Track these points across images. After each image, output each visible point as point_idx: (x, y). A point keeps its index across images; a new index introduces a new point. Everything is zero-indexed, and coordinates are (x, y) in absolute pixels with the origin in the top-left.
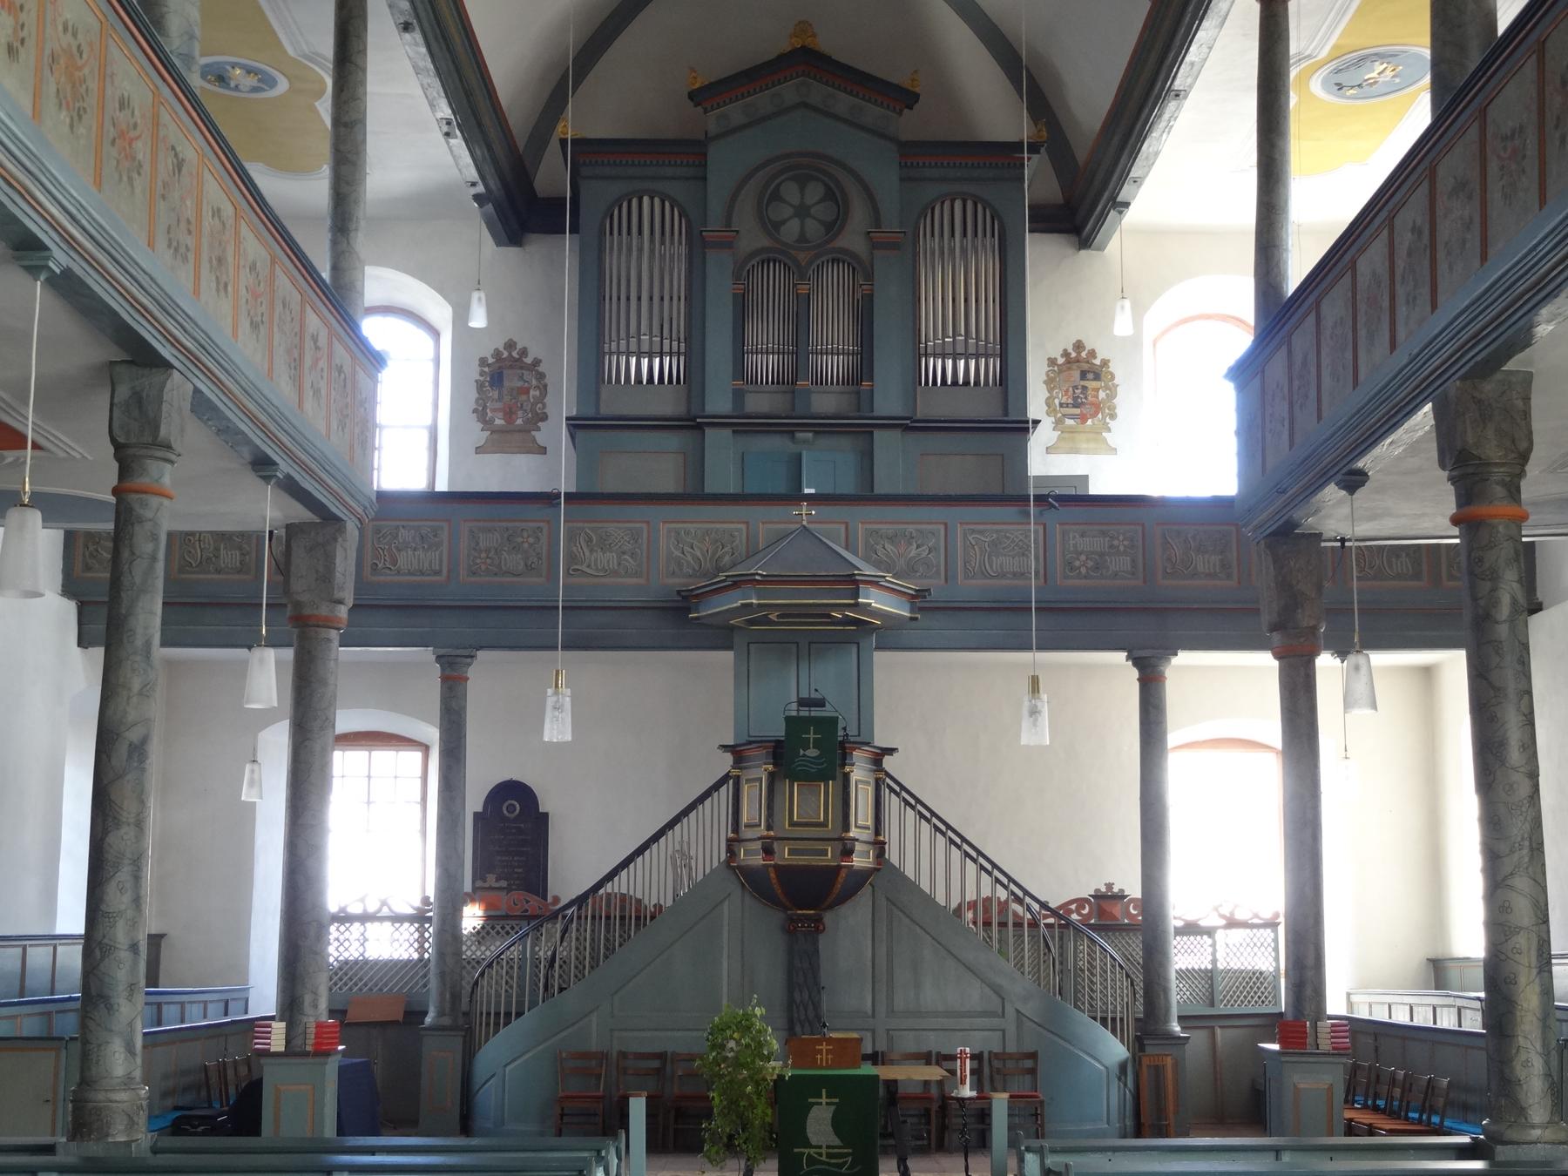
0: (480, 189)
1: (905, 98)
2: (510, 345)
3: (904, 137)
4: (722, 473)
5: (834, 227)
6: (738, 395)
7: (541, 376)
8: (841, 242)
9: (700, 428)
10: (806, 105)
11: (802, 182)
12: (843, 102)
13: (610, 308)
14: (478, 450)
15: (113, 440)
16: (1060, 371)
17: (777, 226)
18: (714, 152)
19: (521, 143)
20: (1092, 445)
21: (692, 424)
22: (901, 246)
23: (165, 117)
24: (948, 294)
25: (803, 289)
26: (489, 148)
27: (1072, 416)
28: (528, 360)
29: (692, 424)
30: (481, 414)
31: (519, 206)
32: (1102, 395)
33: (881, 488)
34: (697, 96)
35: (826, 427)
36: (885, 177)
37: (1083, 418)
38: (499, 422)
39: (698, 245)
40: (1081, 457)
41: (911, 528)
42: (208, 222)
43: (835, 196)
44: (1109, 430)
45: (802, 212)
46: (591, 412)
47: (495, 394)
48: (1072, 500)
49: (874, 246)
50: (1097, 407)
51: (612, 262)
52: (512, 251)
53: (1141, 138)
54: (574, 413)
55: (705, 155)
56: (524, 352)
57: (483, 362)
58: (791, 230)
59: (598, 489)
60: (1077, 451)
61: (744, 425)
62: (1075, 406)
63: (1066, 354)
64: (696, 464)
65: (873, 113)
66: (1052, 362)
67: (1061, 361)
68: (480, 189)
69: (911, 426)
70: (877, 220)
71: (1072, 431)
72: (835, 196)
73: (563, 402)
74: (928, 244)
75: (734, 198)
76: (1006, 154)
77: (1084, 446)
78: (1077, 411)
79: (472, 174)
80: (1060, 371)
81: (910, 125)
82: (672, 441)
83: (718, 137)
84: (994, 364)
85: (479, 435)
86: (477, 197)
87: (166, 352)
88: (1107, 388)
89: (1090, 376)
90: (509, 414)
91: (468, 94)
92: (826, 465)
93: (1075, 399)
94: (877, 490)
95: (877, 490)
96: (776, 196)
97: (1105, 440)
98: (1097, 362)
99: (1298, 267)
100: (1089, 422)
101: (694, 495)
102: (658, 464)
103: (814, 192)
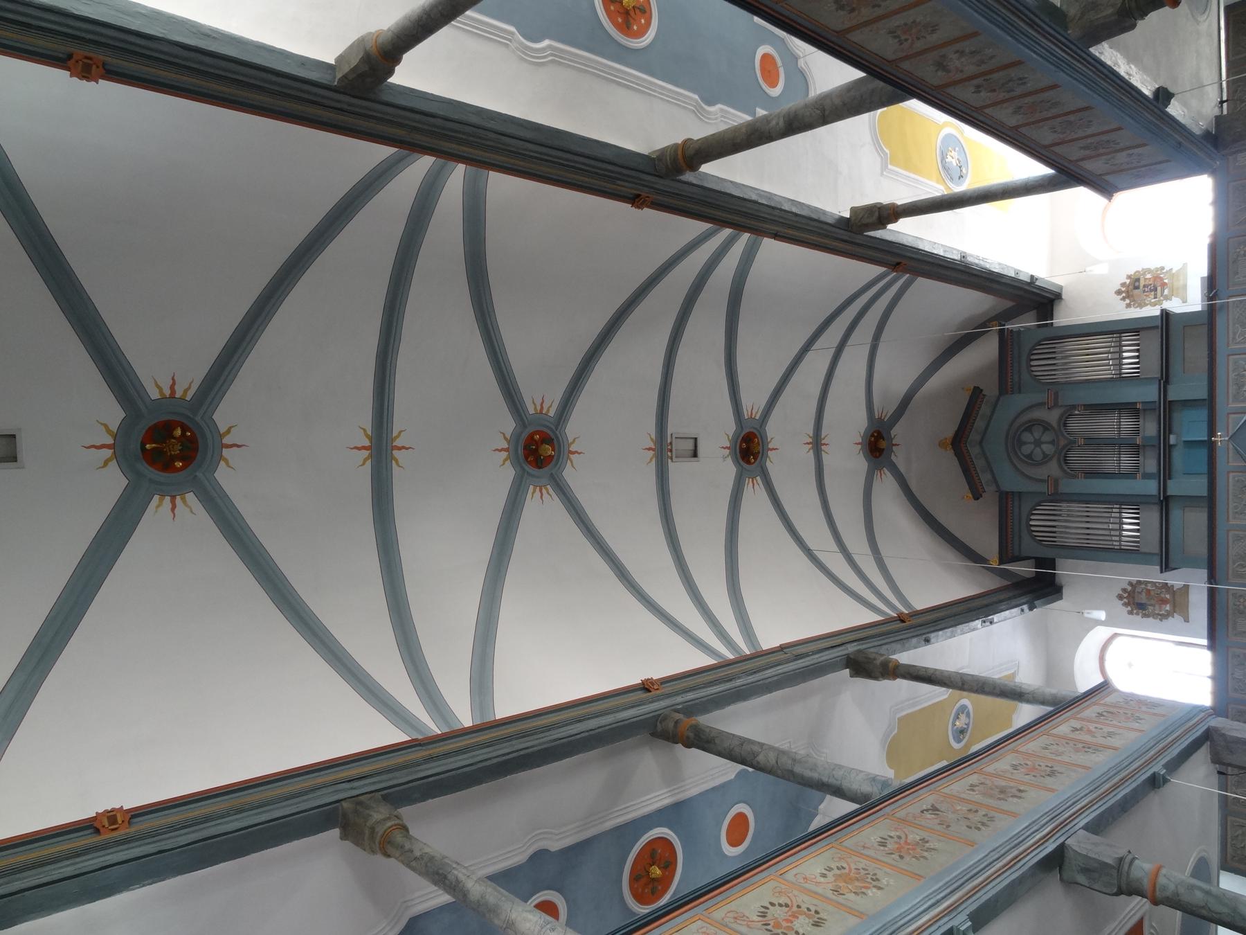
0: (1025, 607)
1: (977, 393)
2: (1120, 597)
3: (996, 392)
4: (1198, 486)
5: (1046, 427)
6: (1147, 476)
7: (1139, 582)
8: (1054, 424)
9: (1167, 498)
10: (981, 443)
11: (1022, 443)
12: (979, 424)
13: (1093, 544)
14: (1187, 620)
15: (1116, 894)
17: (1045, 456)
18: (1007, 486)
19: (1006, 583)
21: (1165, 503)
22: (1055, 389)
23: (901, 814)
24: (1089, 364)
25: (1082, 442)
26: (1001, 601)
27: (1163, 291)
28: (1129, 588)
29: (1165, 503)
30: (1164, 617)
31: (1040, 587)
32: (1149, 276)
33: (1202, 393)
34: (977, 496)
35: (1167, 427)
36: (1018, 401)
37: (1164, 285)
38: (1168, 607)
39: (1057, 497)
40: (1189, 283)
41: (1232, 375)
42: (976, 797)
43: (1030, 426)
45: (1038, 443)
46: (1157, 559)
47: (1151, 608)
48: (1212, 285)
49: (1056, 405)
50: (1157, 278)
51: (1071, 542)
52: (1064, 591)
53: (991, 273)
54: (1158, 568)
55: (1007, 493)
56: (1124, 590)
57: (1130, 613)
58: (1048, 448)
59: (1205, 556)
61: (1166, 472)
62: (1156, 290)
63: (1124, 299)
64: (1189, 501)
65: (985, 409)
66: (1128, 306)
67: (1128, 301)
68: (1025, 607)
69: (1165, 379)
70: (1041, 404)
72: (1030, 426)
73: (1151, 574)
74: (1060, 377)
75: (1030, 478)
76: (1006, 340)
79: (1016, 611)
81: (991, 390)
82: (1176, 514)
83: (998, 486)
84: (1125, 337)
85: (1177, 620)
86: (1031, 609)
87: (1051, 847)
88: (1144, 274)
90: (1164, 602)
91: (970, 610)
92: (1190, 427)
94: (1205, 396)
95: (1205, 396)
96: (1029, 456)
99: (1037, 169)
101: (1210, 501)
102: (1190, 524)
103: (1027, 437)
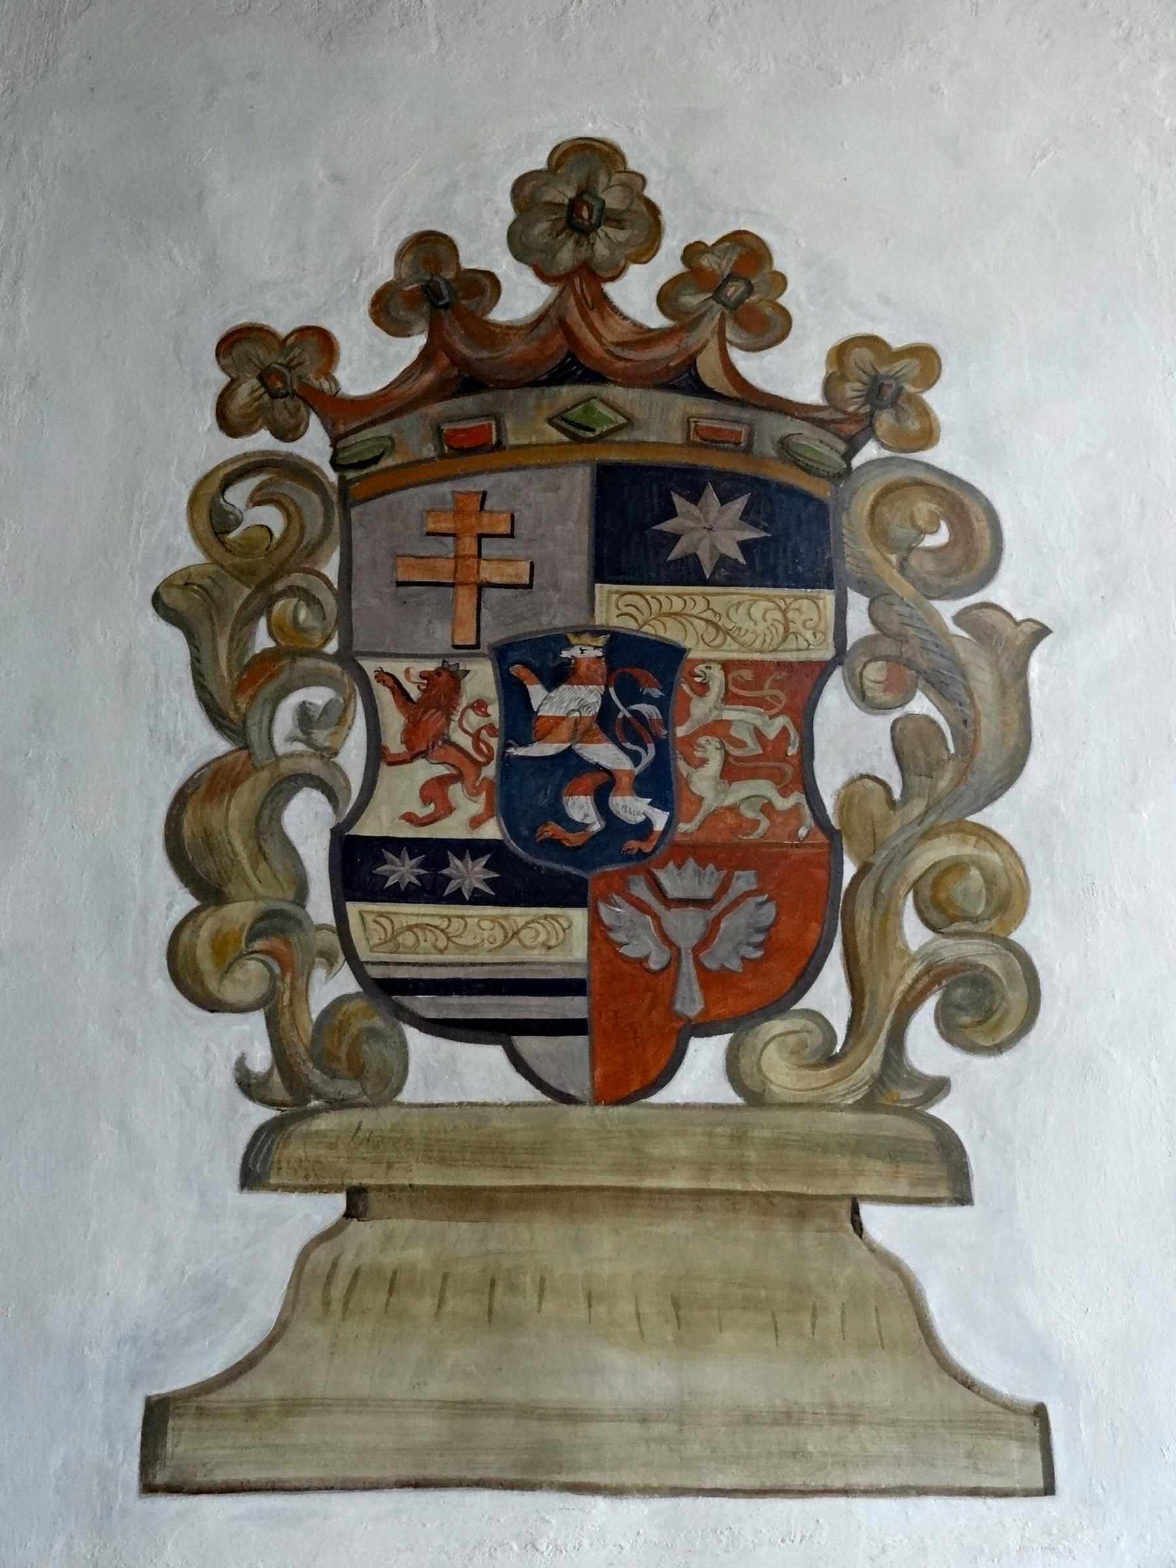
16: (362, 477)
20: (731, 1375)
27: (483, 1006)
32: (850, 741)
44: (948, 1174)
50: (804, 891)
60: (539, 1459)
62: (518, 880)
63: (431, 287)
66: (271, 371)
67: (371, 361)
71: (478, 1181)
77: (632, 1377)
78: (556, 938)
80: (362, 477)
88: (906, 661)
89: (713, 528)
93: (529, 789)
97: (898, 1308)
98: (792, 371)
100: (702, 1072)
